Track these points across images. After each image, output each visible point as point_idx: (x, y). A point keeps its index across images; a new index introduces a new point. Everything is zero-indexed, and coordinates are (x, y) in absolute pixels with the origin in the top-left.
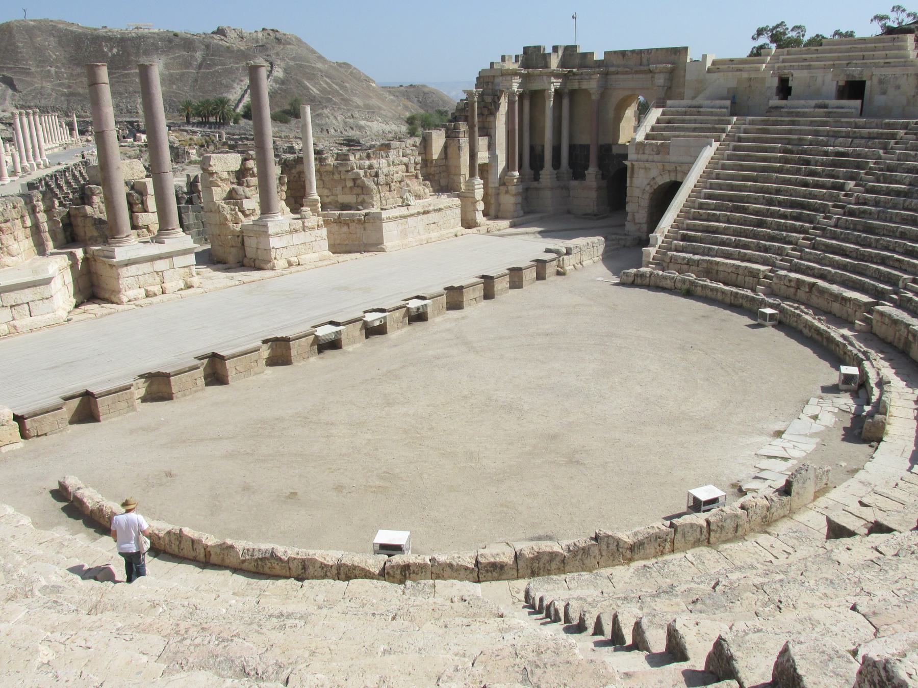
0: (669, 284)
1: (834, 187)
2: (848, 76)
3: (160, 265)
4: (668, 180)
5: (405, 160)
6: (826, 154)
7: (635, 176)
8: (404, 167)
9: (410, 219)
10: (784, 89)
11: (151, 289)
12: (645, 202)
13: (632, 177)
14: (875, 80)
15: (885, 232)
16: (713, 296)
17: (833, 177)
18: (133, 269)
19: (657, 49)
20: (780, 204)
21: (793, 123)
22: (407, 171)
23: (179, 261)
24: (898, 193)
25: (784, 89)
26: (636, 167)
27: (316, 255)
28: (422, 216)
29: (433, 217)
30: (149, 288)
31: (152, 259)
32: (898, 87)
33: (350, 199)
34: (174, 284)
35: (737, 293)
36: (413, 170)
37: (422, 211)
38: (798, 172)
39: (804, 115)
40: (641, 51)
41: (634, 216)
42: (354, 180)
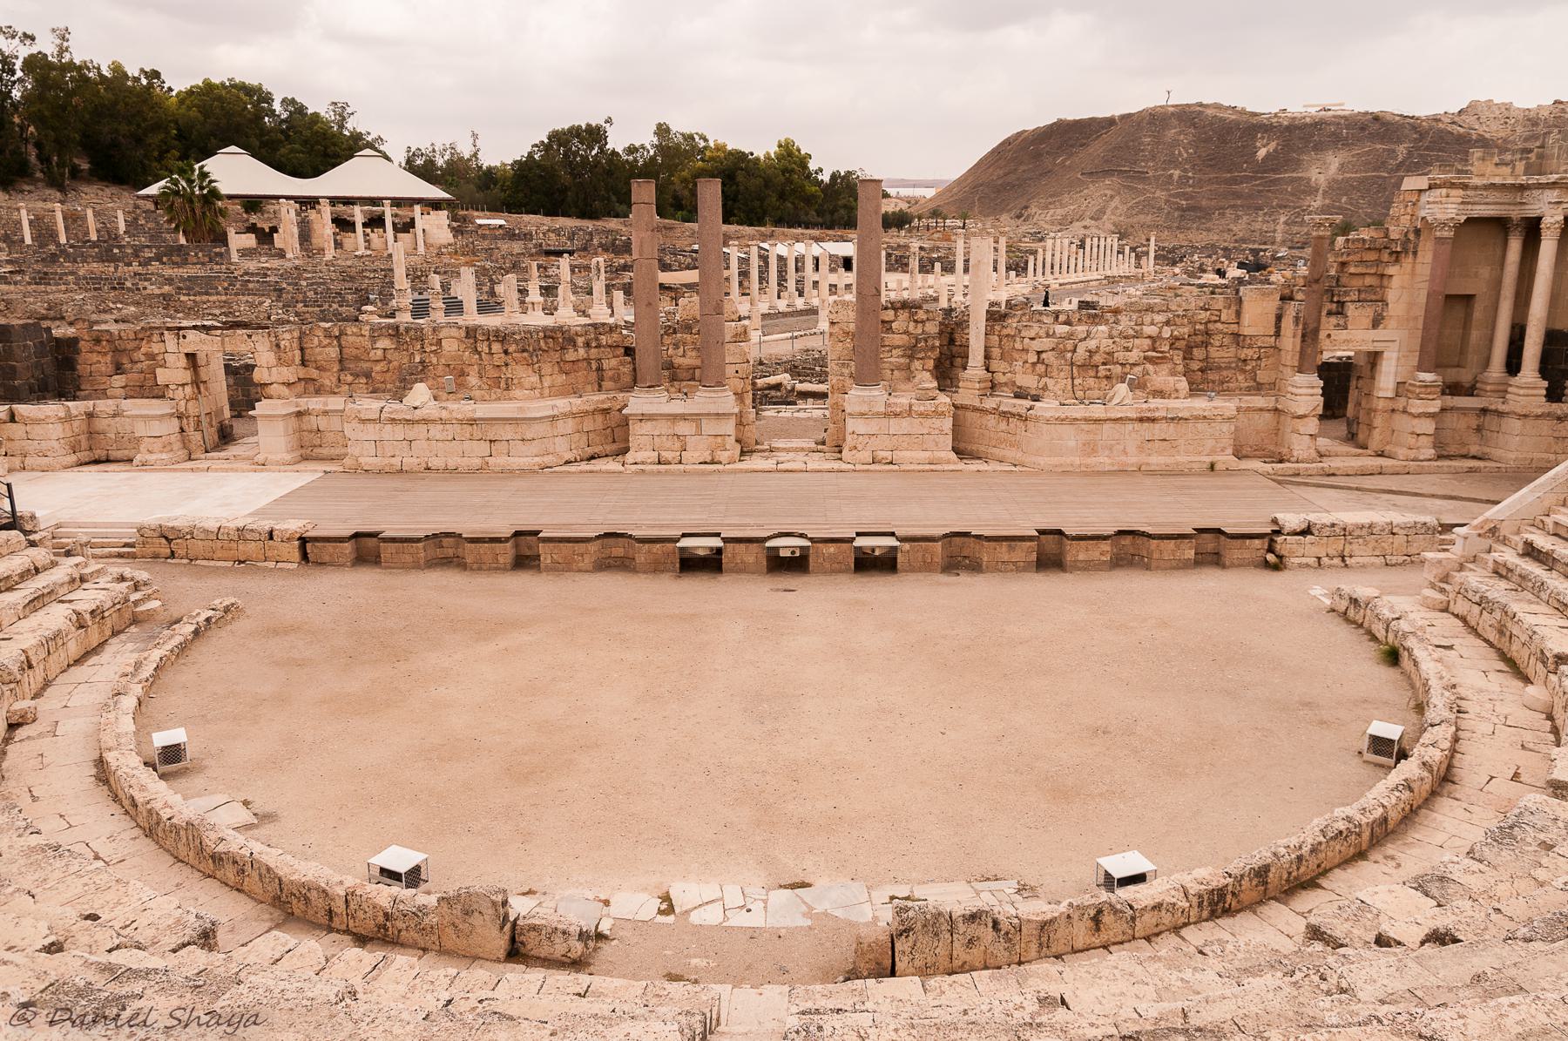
3: (684, 428)
5: (1150, 330)
8: (1148, 341)
9: (1106, 426)
11: (666, 455)
18: (647, 427)
22: (1154, 350)
23: (709, 427)
27: (927, 454)
28: (1137, 426)
29: (1158, 430)
30: (663, 453)
31: (675, 418)
33: (1028, 381)
34: (696, 454)
36: (1166, 348)
37: (1134, 415)
42: (1039, 353)
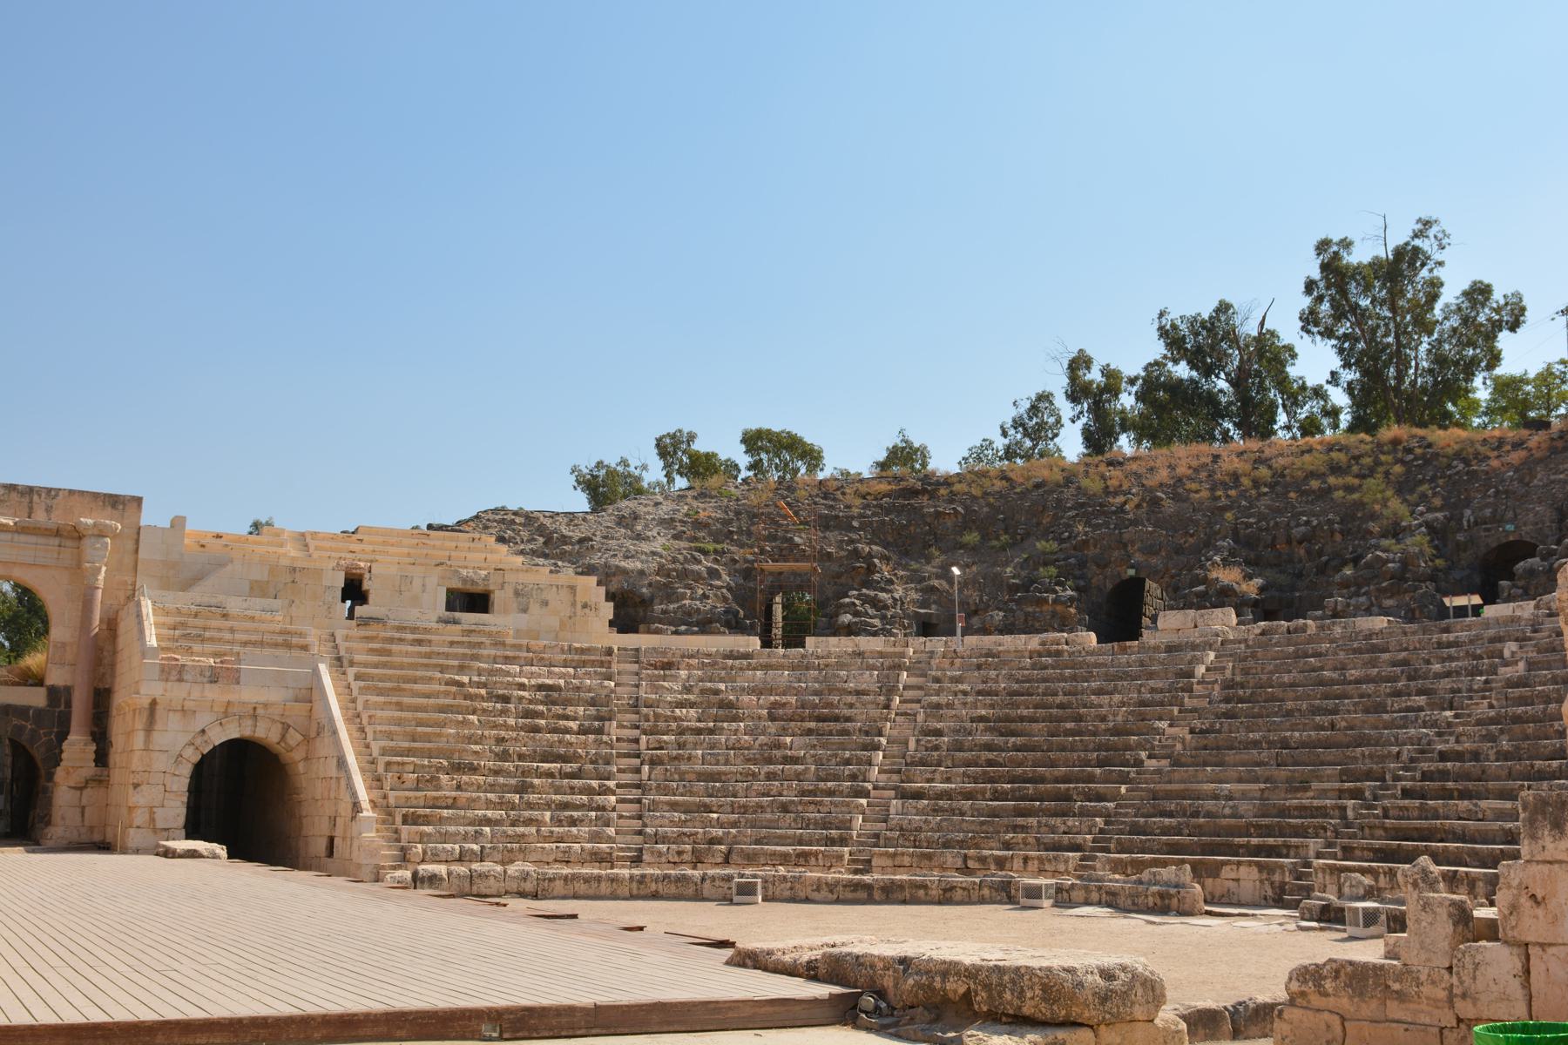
0: (493, 885)
1: (583, 731)
2: (465, 580)
4: (235, 735)
6: (522, 687)
7: (159, 726)
10: (354, 591)
12: (181, 784)
13: (149, 729)
14: (509, 591)
15: (739, 777)
16: (591, 892)
17: (567, 718)
19: (71, 492)
20: (521, 757)
21: (419, 642)
24: (699, 732)
25: (354, 591)
26: (159, 709)
32: (545, 603)
35: (643, 876)
38: (504, 712)
39: (426, 631)
40: (31, 490)
41: (152, 813)
